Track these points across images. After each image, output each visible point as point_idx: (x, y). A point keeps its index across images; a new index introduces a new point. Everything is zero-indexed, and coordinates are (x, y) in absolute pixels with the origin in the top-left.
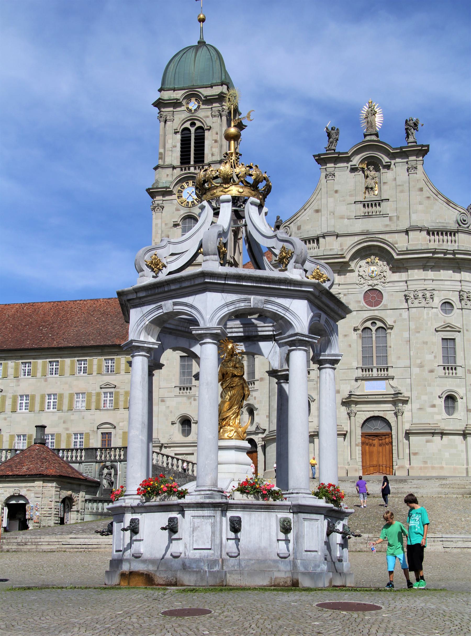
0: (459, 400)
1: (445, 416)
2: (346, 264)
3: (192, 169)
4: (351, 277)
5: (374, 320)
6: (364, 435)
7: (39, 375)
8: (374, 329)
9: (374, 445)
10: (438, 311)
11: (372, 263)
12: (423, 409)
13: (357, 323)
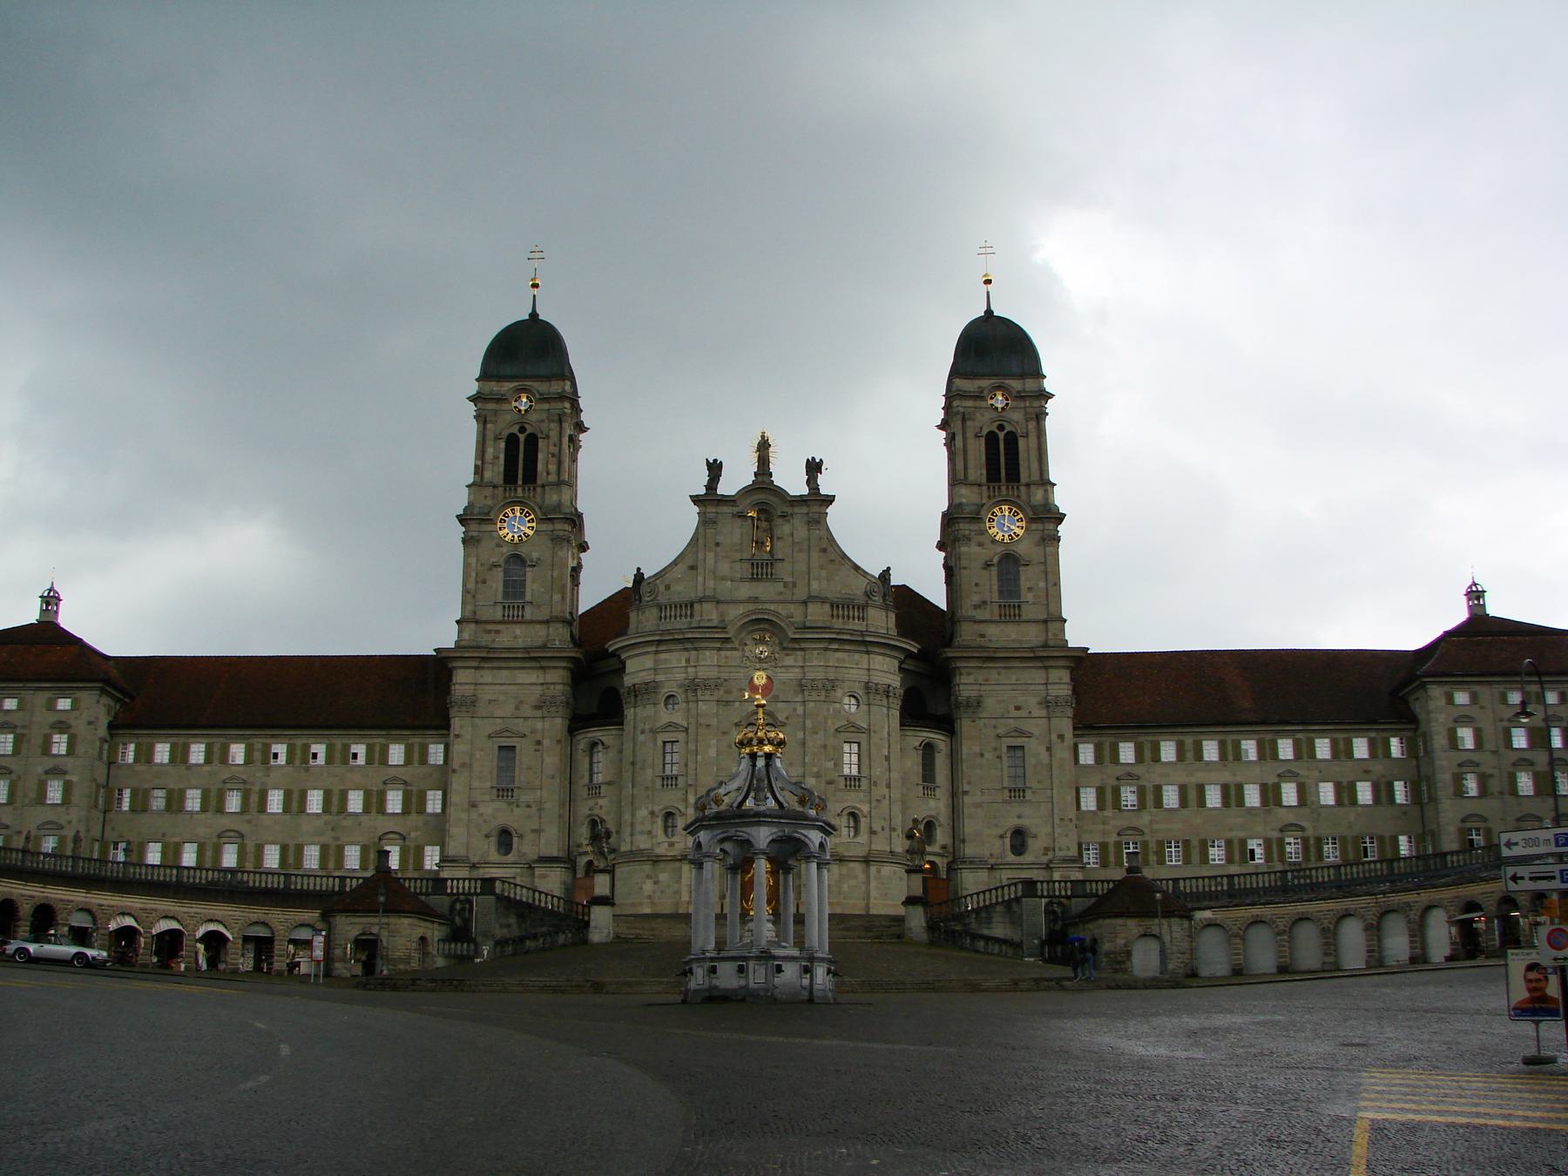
0: (862, 819)
2: (727, 640)
7: (297, 762)
11: (762, 641)
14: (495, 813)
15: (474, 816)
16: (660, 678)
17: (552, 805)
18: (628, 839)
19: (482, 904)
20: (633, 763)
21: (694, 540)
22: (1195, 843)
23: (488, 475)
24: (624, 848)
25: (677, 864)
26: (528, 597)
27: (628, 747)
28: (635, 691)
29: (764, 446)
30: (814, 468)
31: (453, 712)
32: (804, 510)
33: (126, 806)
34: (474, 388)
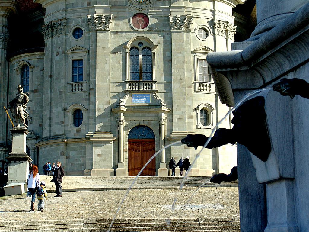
8: (141, 48)
9: (139, 151)
16: (70, 16)
18: (48, 128)
20: (51, 76)
24: (45, 135)
25: (83, 145)
27: (47, 65)
28: (51, 27)
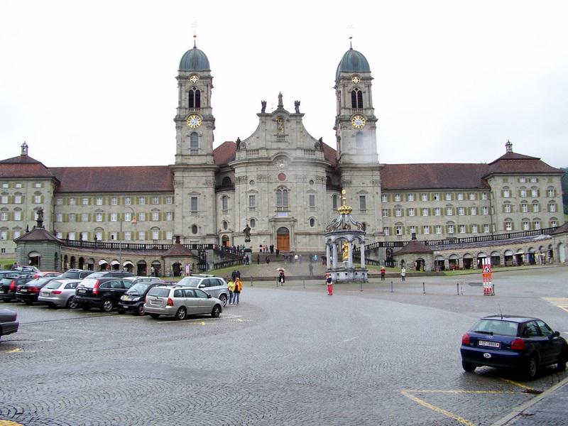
1: (310, 227)
3: (194, 110)
4: (273, 168)
5: (282, 187)
6: (278, 235)
7: (121, 204)
10: (308, 184)
12: (302, 225)
13: (275, 188)
14: (192, 220)
15: (184, 221)
17: (211, 217)
19: (209, 253)
21: (258, 128)
22: (419, 227)
23: (183, 105)
24: (237, 231)
26: (199, 147)
27: (237, 198)
28: (239, 179)
29: (280, 96)
30: (297, 104)
31: (175, 186)
32: (295, 118)
33: (61, 220)
34: (177, 74)
